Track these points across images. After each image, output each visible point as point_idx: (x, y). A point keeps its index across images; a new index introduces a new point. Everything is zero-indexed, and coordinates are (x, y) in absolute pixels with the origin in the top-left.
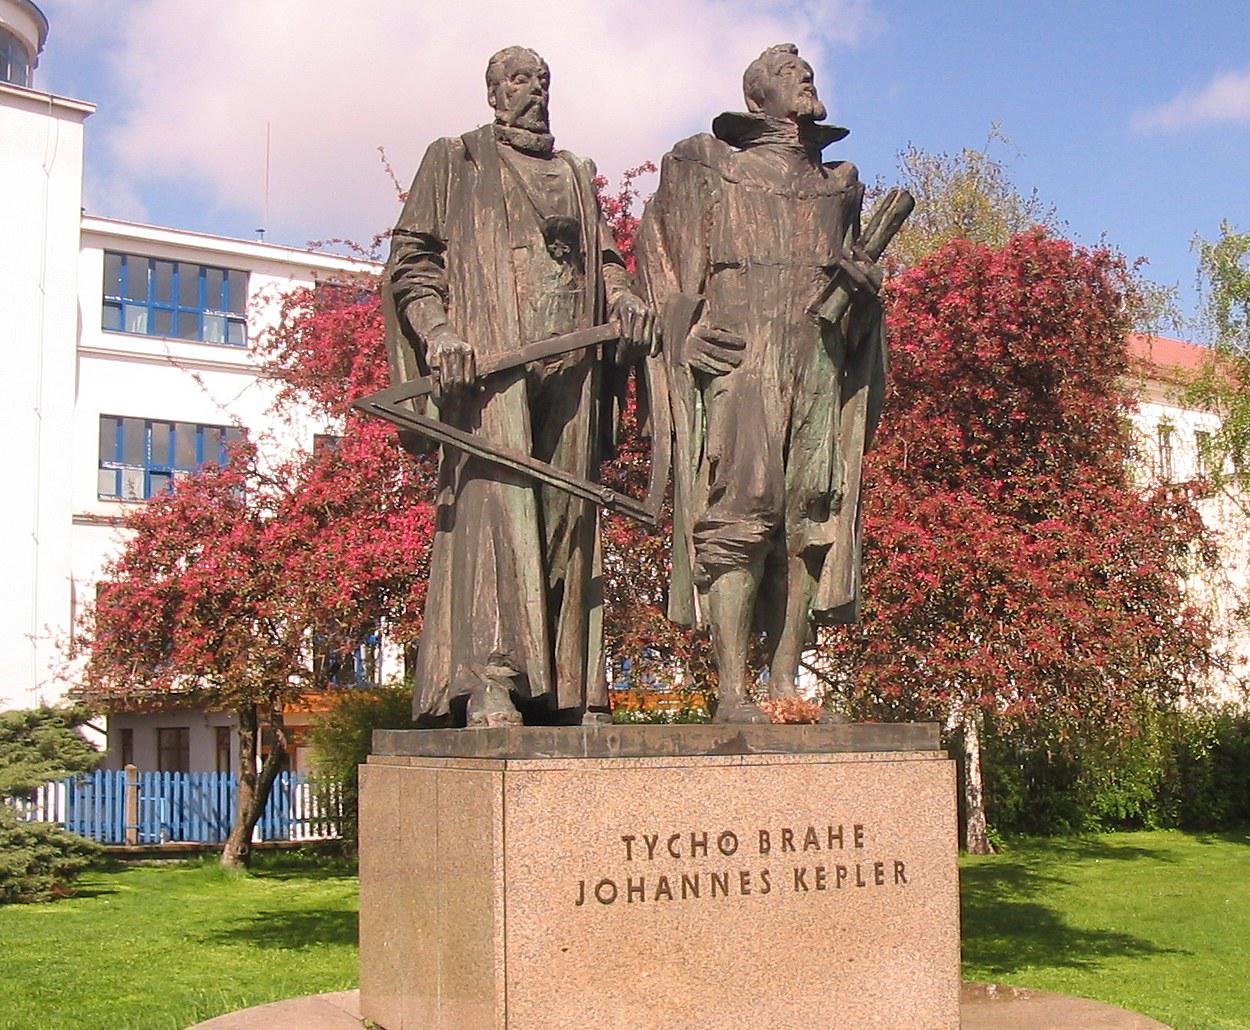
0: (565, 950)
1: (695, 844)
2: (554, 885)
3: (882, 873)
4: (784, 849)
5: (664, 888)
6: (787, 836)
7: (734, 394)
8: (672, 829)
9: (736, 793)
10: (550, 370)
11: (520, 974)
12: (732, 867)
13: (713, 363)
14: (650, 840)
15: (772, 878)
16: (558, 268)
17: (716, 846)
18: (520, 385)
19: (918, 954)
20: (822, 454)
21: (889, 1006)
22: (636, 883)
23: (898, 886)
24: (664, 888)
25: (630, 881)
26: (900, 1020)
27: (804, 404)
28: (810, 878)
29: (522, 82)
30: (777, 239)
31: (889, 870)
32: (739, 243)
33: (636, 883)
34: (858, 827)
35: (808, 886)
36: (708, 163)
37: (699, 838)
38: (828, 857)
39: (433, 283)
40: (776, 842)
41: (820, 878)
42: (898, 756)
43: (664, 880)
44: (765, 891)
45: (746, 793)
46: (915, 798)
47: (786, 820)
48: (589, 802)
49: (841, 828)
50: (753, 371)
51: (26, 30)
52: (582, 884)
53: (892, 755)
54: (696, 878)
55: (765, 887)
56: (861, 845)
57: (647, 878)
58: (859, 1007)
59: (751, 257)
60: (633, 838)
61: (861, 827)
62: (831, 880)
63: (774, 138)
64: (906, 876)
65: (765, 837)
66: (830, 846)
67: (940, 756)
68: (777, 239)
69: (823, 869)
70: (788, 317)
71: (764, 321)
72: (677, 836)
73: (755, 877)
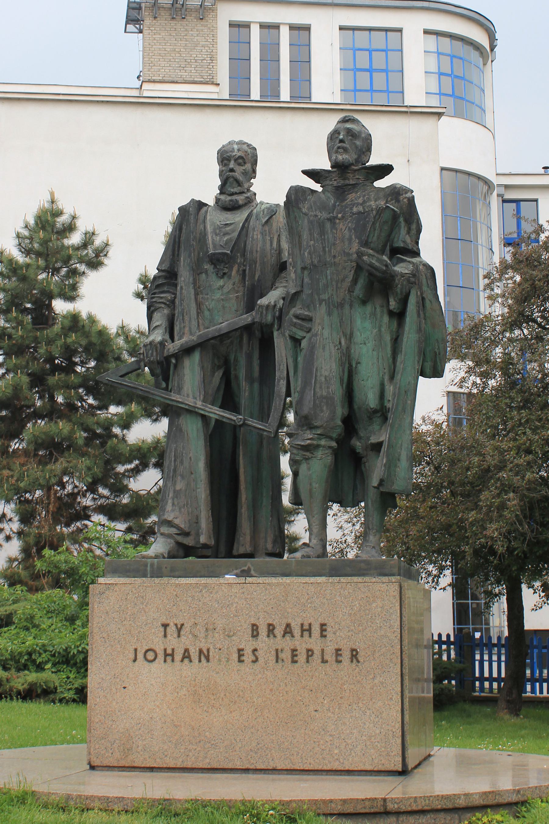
0: (125, 688)
2: (119, 649)
4: (268, 636)
5: (186, 655)
6: (271, 629)
9: (236, 600)
11: (98, 700)
14: (179, 626)
15: (259, 653)
16: (221, 282)
22: (169, 651)
24: (186, 655)
25: (165, 650)
26: (353, 754)
27: (355, 351)
28: (286, 655)
30: (324, 248)
31: (346, 655)
33: (169, 651)
34: (322, 625)
38: (302, 644)
40: (263, 631)
42: (360, 579)
43: (187, 650)
44: (256, 661)
47: (271, 618)
49: (310, 625)
52: (136, 650)
53: (355, 579)
54: (208, 650)
55: (254, 658)
56: (325, 636)
58: (322, 742)
59: (312, 261)
61: (325, 625)
62: (302, 658)
64: (360, 659)
65: (255, 628)
66: (302, 636)
68: (324, 248)
69: (296, 650)
70: (335, 297)
71: (321, 301)
73: (248, 652)
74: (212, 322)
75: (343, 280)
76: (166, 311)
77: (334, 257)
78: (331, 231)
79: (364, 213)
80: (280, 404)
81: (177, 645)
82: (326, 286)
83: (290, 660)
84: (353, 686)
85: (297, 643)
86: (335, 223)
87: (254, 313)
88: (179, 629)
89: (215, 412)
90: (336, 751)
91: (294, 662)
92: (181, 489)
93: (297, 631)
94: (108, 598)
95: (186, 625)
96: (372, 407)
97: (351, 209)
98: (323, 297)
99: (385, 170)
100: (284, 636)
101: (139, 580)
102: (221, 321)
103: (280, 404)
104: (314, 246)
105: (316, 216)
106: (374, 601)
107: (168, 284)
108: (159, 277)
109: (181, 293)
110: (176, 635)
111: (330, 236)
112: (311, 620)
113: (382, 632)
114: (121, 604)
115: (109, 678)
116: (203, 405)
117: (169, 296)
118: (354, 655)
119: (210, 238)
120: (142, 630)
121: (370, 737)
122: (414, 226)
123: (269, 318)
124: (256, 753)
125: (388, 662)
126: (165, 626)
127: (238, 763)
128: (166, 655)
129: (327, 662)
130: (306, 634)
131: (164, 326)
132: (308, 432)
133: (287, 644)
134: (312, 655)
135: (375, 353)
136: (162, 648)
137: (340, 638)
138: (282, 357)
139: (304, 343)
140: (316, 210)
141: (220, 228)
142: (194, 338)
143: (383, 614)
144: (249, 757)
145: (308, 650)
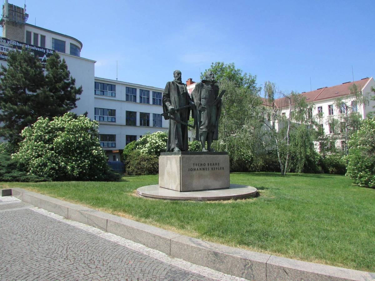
6: (211, 164)
28: (213, 169)
31: (222, 168)
38: (216, 167)
43: (198, 169)
51: (80, 46)
62: (216, 169)
73: (207, 168)
93: (215, 164)
126: (194, 164)
133: (213, 167)
137: (221, 166)
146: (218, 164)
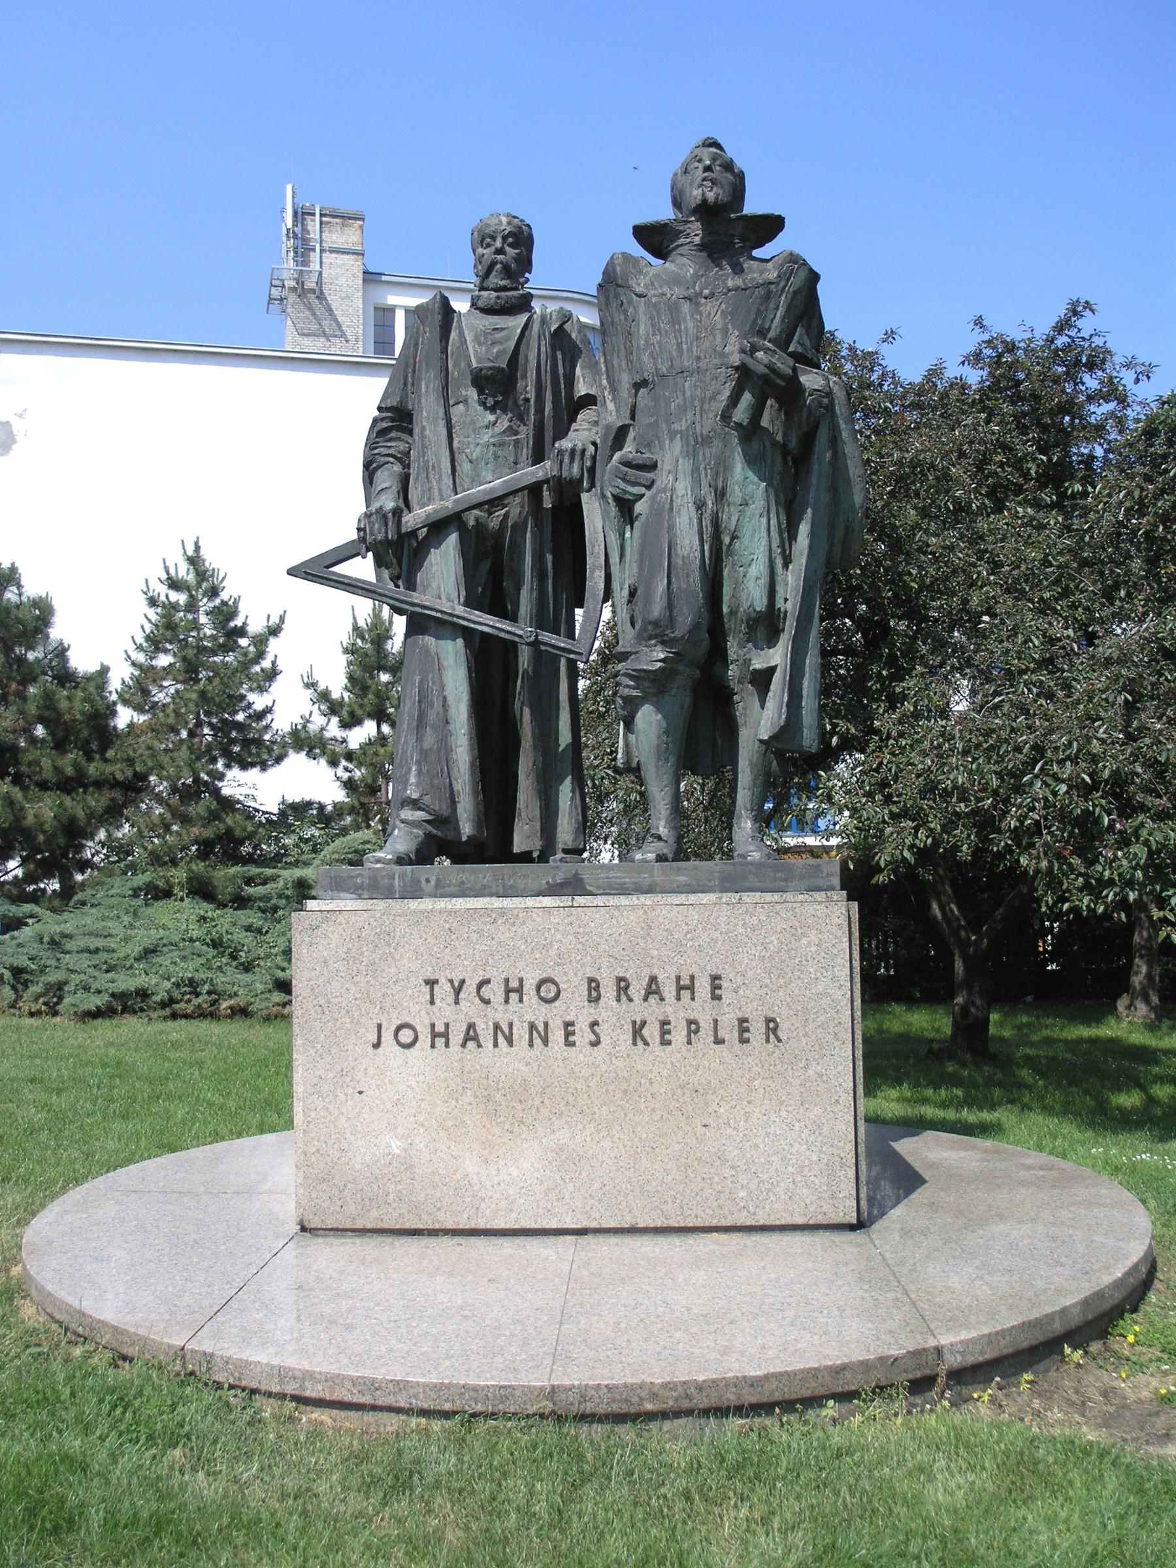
0: (360, 1093)
1: (508, 991)
2: (349, 1026)
3: (747, 1030)
5: (471, 1035)
7: (647, 519)
8: (482, 973)
9: (559, 936)
10: (494, 523)
11: (313, 1114)
12: (555, 1016)
13: (629, 489)
14: (456, 984)
16: (492, 418)
17: (533, 993)
18: (453, 539)
19: (797, 1124)
20: (757, 569)
21: (757, 1180)
22: (440, 1028)
23: (770, 1046)
24: (471, 1035)
25: (433, 1026)
27: (730, 518)
28: (652, 1032)
29: (488, 245)
30: (679, 345)
31: (757, 1029)
32: (645, 358)
33: (440, 1028)
34: (715, 978)
35: (649, 1040)
36: (620, 282)
37: (514, 984)
39: (391, 451)
40: (608, 990)
41: (664, 1032)
42: (776, 897)
43: (471, 1026)
45: (571, 937)
46: (794, 945)
47: (622, 966)
48: (389, 945)
49: (692, 978)
50: (664, 490)
52: (379, 1026)
53: (768, 897)
54: (511, 1025)
55: (593, 1038)
56: (719, 998)
57: (550, 1022)
58: (716, 1179)
60: (436, 982)
62: (678, 1035)
63: (682, 241)
64: (780, 1034)
65: (593, 985)
67: (835, 898)
68: (679, 345)
72: (488, 982)
74: (476, 480)
75: (713, 398)
76: (397, 468)
77: (698, 358)
78: (692, 316)
79: (745, 289)
80: (595, 608)
81: (456, 1017)
82: (683, 409)
83: (658, 1039)
84: (769, 1082)
85: (669, 1009)
86: (698, 304)
87: (548, 464)
88: (457, 992)
89: (485, 622)
90: (742, 1194)
91: (665, 1043)
92: (431, 749)
93: (669, 990)
94: (326, 936)
95: (468, 982)
96: (758, 609)
97: (724, 282)
98: (676, 426)
99: (771, 226)
100: (645, 1000)
101: (380, 905)
102: (490, 478)
103: (595, 608)
104: (660, 343)
105: (663, 294)
106: (804, 935)
107: (399, 429)
108: (382, 419)
109: (423, 437)
110: (451, 999)
111: (691, 325)
112: (694, 970)
113: (820, 988)
114: (350, 946)
115: (331, 1075)
116: (465, 611)
117: (402, 446)
118: (772, 1027)
119: (470, 349)
120: (389, 992)
121: (802, 1167)
122: (815, 323)
123: (576, 470)
124: (600, 1201)
125: (830, 1038)
127: (568, 1220)
128: (435, 1035)
129: (722, 1042)
130: (686, 994)
131: (395, 488)
132: (659, 648)
133: (652, 1012)
134: (697, 1031)
135: (764, 520)
136: (427, 1022)
137: (745, 999)
138: (595, 532)
139: (639, 507)
140: (661, 287)
141: (486, 334)
142: (449, 504)
143: (820, 957)
144: (588, 1208)
145: (690, 1022)
146: (703, 987)
